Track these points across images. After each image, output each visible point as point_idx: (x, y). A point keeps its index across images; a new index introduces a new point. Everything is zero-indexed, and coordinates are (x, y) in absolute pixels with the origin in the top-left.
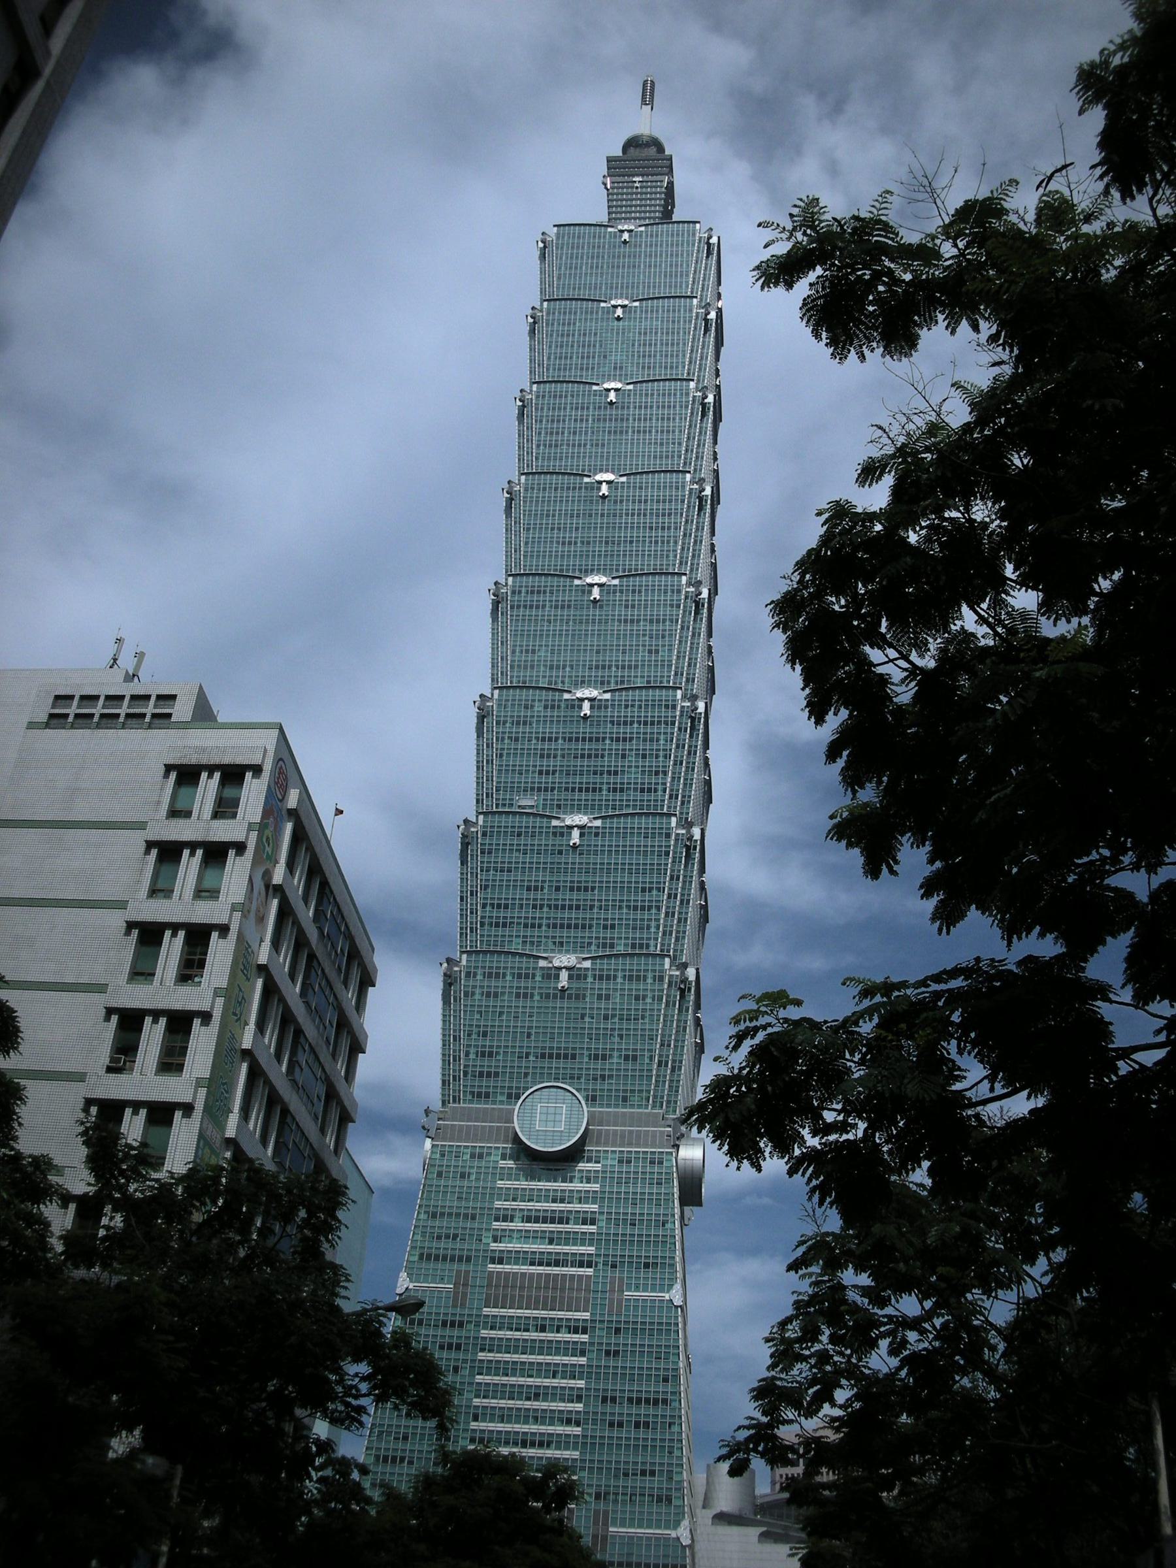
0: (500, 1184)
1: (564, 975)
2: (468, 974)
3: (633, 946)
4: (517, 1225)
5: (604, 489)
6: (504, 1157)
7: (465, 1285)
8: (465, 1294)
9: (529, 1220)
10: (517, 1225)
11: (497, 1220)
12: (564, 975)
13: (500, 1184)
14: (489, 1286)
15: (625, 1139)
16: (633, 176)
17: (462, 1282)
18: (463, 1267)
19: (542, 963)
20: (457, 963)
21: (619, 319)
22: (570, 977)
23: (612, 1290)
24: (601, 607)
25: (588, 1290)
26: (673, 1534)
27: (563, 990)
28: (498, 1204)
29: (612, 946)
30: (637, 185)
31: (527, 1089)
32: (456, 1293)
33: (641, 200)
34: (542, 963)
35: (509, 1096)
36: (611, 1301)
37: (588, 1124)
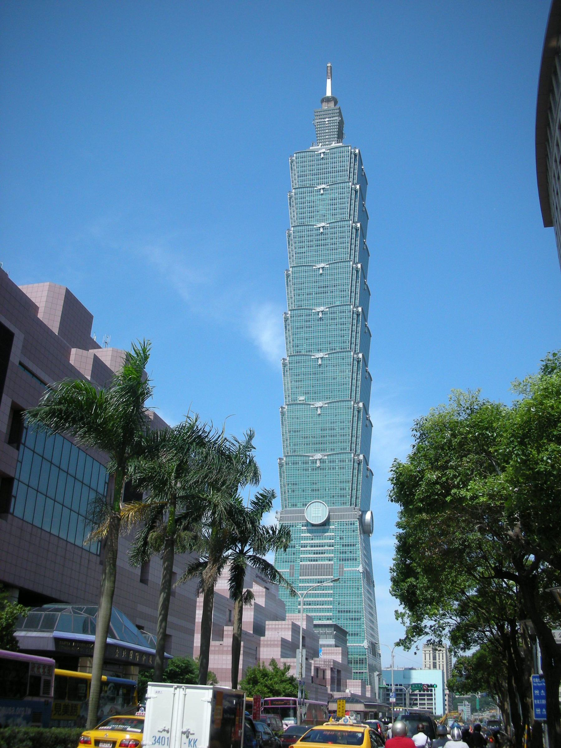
0: (302, 535)
1: (318, 462)
2: (286, 464)
3: (341, 449)
4: (308, 548)
5: (321, 271)
6: (303, 526)
7: (293, 569)
8: (293, 573)
9: (312, 547)
10: (308, 548)
11: (302, 547)
12: (318, 462)
13: (302, 535)
14: (301, 569)
15: (342, 517)
16: (325, 118)
17: (292, 568)
18: (292, 564)
19: (311, 458)
20: (283, 459)
21: (322, 194)
22: (320, 462)
23: (340, 568)
24: (323, 320)
25: (332, 568)
26: (362, 645)
27: (318, 467)
28: (302, 542)
29: (334, 449)
30: (327, 122)
31: (308, 502)
32: (290, 572)
33: (329, 129)
34: (311, 458)
35: (303, 505)
36: (340, 571)
37: (329, 513)
